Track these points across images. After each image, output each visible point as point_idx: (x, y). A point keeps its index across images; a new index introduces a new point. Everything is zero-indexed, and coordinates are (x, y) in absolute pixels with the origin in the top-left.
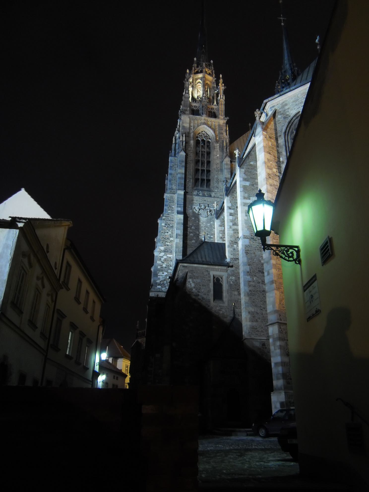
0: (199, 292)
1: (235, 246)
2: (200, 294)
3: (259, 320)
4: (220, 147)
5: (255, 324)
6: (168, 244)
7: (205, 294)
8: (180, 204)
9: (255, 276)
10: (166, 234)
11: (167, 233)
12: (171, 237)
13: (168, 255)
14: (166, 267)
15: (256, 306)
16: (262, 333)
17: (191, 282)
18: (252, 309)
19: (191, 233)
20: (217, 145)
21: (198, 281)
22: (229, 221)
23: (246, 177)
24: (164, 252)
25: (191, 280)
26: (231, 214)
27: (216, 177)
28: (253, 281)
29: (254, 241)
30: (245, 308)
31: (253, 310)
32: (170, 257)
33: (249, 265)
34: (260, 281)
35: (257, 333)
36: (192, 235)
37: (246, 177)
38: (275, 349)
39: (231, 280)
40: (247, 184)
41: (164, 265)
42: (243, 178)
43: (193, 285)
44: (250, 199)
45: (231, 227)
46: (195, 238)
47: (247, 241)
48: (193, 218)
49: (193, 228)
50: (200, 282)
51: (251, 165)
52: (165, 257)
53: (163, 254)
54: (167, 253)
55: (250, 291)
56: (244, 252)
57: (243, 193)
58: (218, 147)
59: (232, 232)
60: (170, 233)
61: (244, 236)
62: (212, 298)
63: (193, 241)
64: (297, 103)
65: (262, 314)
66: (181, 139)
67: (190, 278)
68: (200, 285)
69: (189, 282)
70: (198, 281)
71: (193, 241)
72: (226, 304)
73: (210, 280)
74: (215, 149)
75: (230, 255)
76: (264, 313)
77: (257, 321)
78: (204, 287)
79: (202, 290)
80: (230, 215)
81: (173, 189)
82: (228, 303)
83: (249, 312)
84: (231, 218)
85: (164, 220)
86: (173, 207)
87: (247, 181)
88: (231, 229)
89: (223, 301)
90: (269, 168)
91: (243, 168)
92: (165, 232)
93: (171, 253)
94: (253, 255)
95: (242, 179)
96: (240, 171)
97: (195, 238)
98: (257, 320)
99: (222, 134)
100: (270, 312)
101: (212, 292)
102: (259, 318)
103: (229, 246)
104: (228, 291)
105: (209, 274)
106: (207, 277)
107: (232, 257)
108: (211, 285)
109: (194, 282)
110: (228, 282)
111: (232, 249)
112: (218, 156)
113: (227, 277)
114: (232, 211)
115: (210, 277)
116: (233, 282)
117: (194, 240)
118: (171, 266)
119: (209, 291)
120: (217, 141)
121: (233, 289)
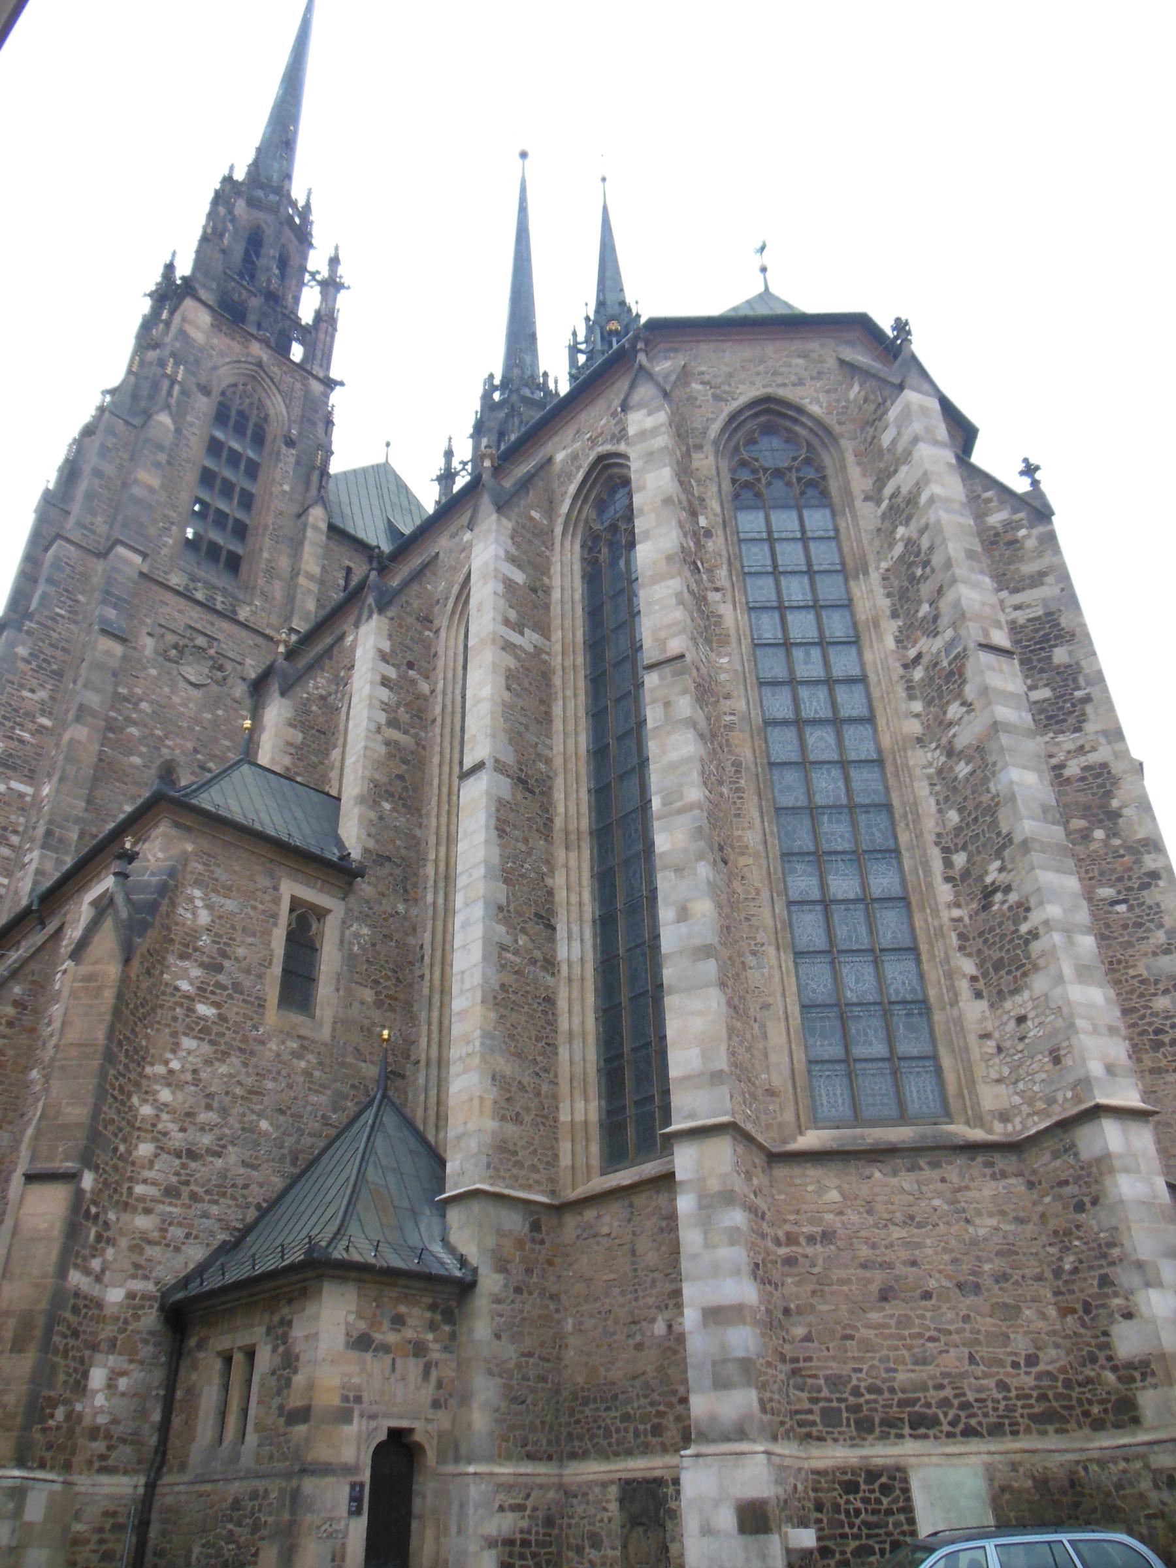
0: (224, 954)
1: (387, 806)
2: (227, 964)
3: (527, 1119)
4: (298, 463)
5: (511, 1129)
6: (26, 736)
7: (248, 971)
8: (118, 598)
9: (523, 931)
10: (25, 693)
11: (33, 691)
12: (43, 712)
13: (14, 784)
15: (519, 1056)
16: (536, 1176)
17: (199, 903)
18: (504, 1065)
19: (135, 723)
20: (290, 456)
21: (230, 905)
22: (378, 704)
23: (513, 550)
25: (197, 893)
26: (385, 682)
27: (266, 555)
28: (516, 953)
29: (528, 795)
30: (482, 1055)
31: (508, 1072)
32: (21, 795)
33: (506, 881)
34: (537, 954)
35: (515, 1171)
36: (133, 730)
37: (516, 553)
38: (708, 1245)
39: (357, 935)
40: (519, 577)
42: (507, 552)
43: (204, 918)
44: (522, 634)
45: (379, 730)
46: (144, 750)
47: (505, 787)
48: (154, 672)
49: (144, 705)
50: (233, 914)
51: (532, 519)
54: (10, 773)
55: (503, 986)
56: (493, 822)
57: (502, 601)
58: (292, 460)
59: (382, 750)
60: (42, 694)
61: (497, 761)
62: (272, 994)
63: (136, 760)
64: (761, 368)
65: (538, 1094)
66: (169, 371)
67: (198, 883)
68: (233, 928)
69: (191, 899)
70: (230, 905)
71: (136, 760)
72: (326, 1033)
73: (275, 916)
74: (278, 460)
75: (364, 837)
76: (545, 1088)
77: (517, 1119)
78: (250, 940)
79: (241, 952)
80: (383, 684)
81: (93, 532)
82: (334, 1030)
83: (494, 1078)
84: (384, 694)
85: (29, 633)
86: (81, 598)
87: (519, 567)
88: (379, 738)
89: (312, 1016)
91: (508, 518)
92: (22, 686)
94: (521, 846)
95: (502, 553)
96: (498, 520)
97: (144, 750)
98: (518, 1114)
99: (314, 424)
100: (686, 1078)
101: (277, 969)
102: (528, 1110)
103: (361, 800)
104: (338, 980)
105: (276, 888)
106: (267, 897)
107: (371, 844)
108: (279, 936)
109: (209, 907)
110: (342, 942)
111: (373, 815)
112: (286, 488)
113: (344, 922)
114: (392, 673)
115: (277, 901)
116: (361, 947)
117: (141, 755)
118: (15, 832)
119: (267, 963)
120: (290, 443)
121: (356, 977)
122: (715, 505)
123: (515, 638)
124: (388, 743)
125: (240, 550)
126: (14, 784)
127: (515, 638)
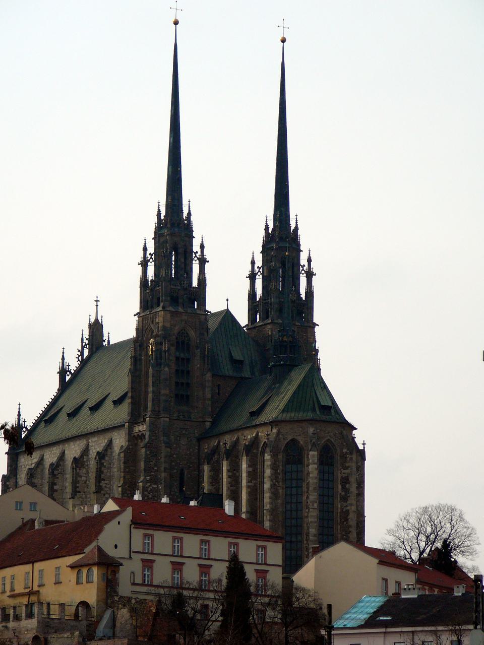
13: (154, 486)
14: (151, 498)
20: (198, 352)
24: (150, 482)
32: (155, 488)
40: (251, 469)
41: (150, 496)
45: (229, 489)
48: (175, 445)
49: (174, 456)
52: (151, 487)
53: (149, 484)
58: (199, 354)
84: (229, 479)
90: (272, 480)
93: (156, 483)
120: (197, 348)
122: (281, 467)
123: (250, 484)
124: (231, 491)
125: (189, 393)
126: (154, 486)
127: (250, 484)
